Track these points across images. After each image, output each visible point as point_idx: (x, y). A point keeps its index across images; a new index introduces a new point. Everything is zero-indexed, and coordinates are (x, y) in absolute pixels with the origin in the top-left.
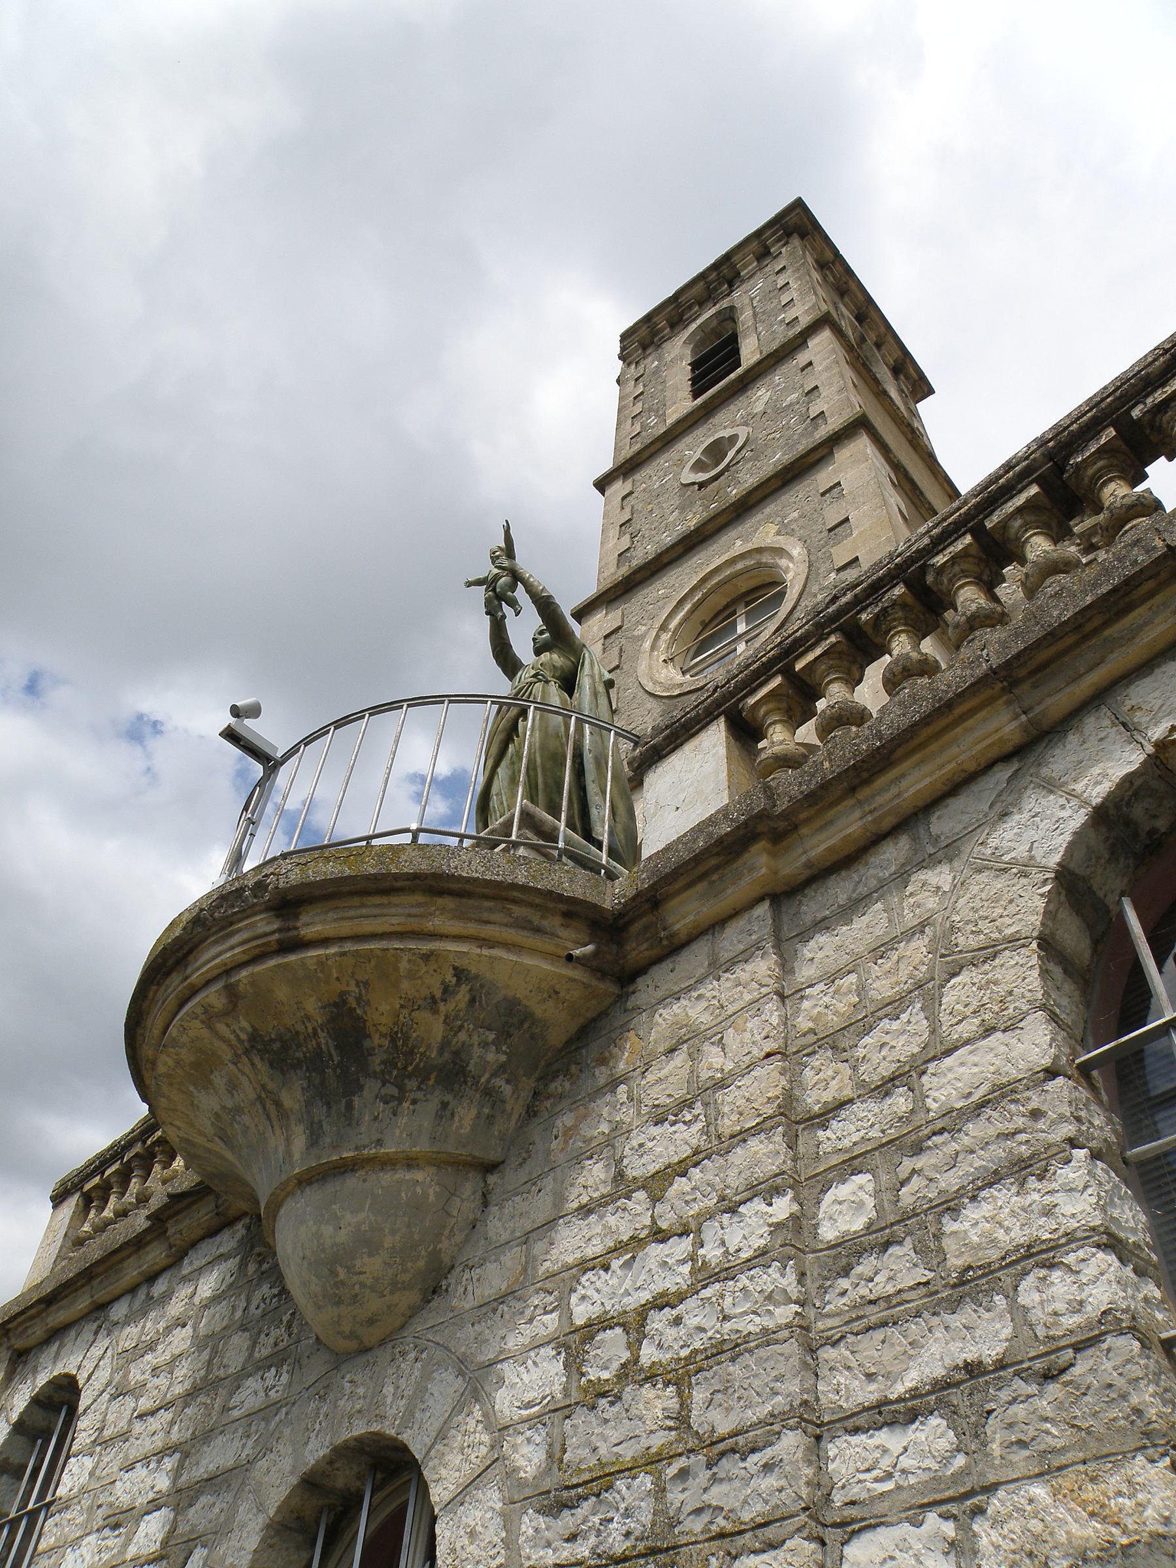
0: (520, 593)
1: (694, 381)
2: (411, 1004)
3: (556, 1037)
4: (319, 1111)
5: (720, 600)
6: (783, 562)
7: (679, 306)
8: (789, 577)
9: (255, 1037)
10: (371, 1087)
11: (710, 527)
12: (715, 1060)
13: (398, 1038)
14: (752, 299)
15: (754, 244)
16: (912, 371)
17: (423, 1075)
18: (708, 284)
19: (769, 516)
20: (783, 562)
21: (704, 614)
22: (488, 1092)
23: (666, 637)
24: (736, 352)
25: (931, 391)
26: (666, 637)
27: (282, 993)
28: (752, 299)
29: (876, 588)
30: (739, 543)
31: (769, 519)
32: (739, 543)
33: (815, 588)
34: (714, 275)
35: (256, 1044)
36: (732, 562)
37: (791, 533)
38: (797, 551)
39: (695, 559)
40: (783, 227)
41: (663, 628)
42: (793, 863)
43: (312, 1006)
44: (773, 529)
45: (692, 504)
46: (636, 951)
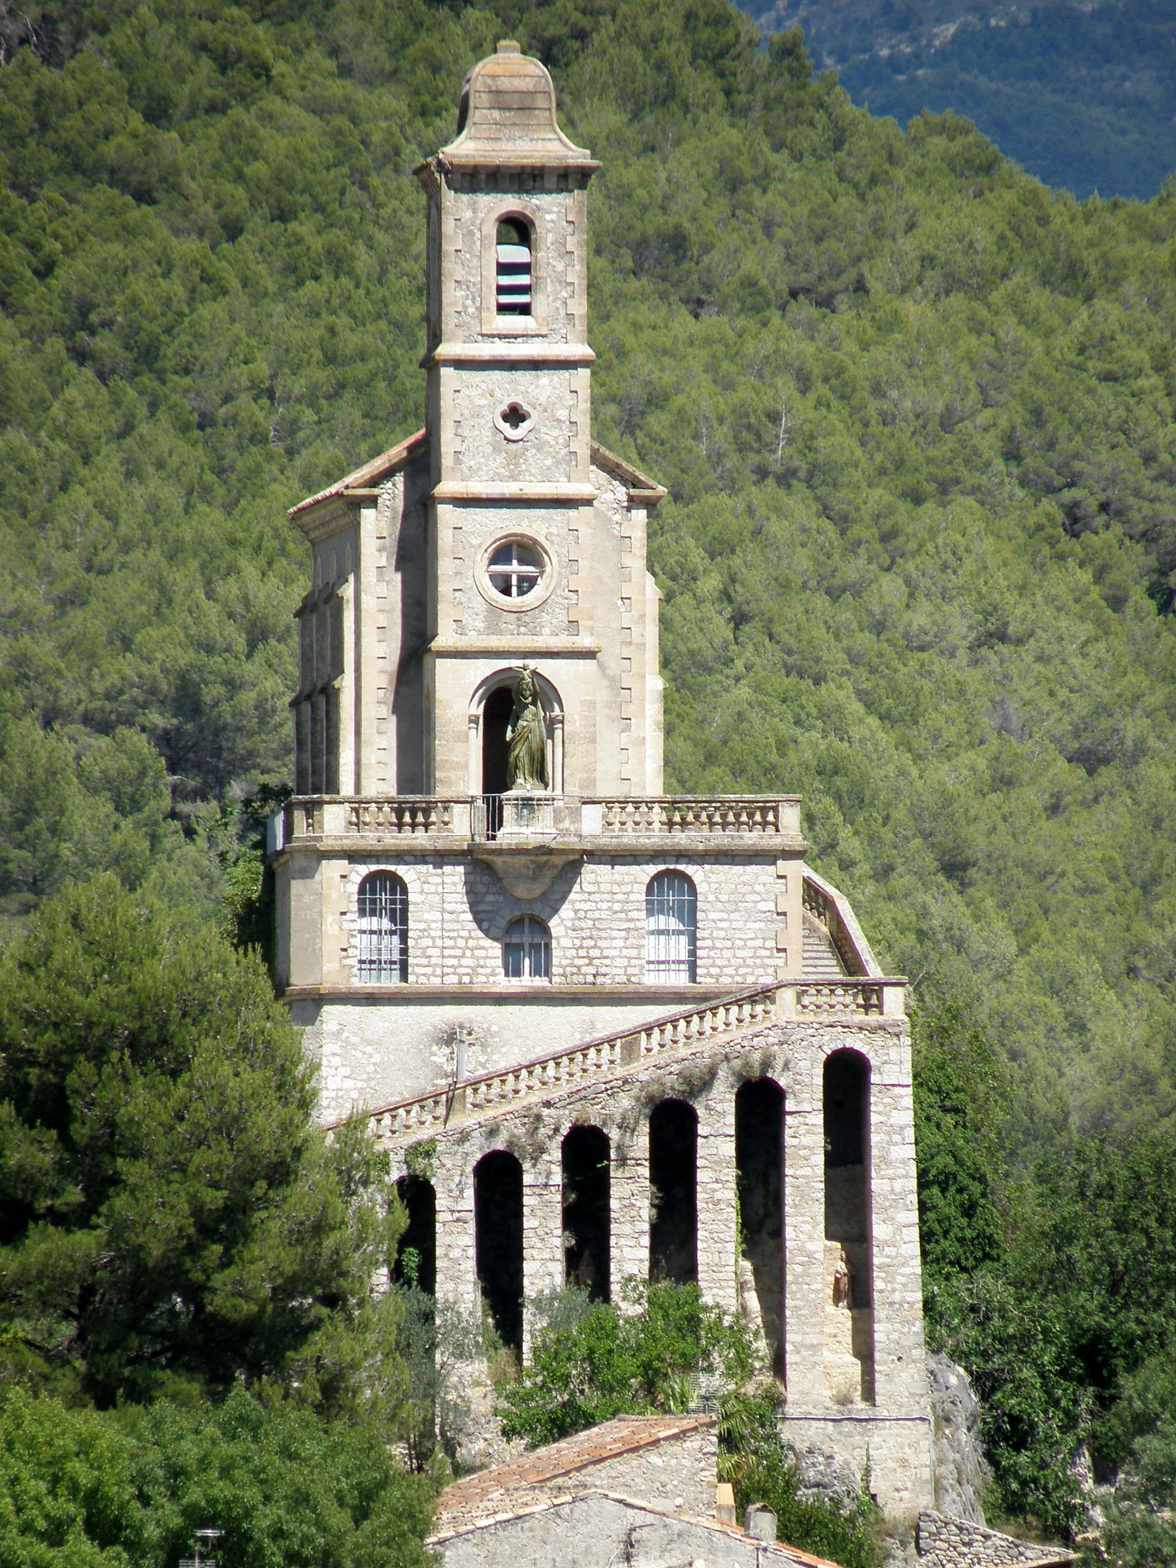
23: (486, 555)
36: (522, 535)
37: (552, 543)
38: (554, 561)
44: (544, 531)
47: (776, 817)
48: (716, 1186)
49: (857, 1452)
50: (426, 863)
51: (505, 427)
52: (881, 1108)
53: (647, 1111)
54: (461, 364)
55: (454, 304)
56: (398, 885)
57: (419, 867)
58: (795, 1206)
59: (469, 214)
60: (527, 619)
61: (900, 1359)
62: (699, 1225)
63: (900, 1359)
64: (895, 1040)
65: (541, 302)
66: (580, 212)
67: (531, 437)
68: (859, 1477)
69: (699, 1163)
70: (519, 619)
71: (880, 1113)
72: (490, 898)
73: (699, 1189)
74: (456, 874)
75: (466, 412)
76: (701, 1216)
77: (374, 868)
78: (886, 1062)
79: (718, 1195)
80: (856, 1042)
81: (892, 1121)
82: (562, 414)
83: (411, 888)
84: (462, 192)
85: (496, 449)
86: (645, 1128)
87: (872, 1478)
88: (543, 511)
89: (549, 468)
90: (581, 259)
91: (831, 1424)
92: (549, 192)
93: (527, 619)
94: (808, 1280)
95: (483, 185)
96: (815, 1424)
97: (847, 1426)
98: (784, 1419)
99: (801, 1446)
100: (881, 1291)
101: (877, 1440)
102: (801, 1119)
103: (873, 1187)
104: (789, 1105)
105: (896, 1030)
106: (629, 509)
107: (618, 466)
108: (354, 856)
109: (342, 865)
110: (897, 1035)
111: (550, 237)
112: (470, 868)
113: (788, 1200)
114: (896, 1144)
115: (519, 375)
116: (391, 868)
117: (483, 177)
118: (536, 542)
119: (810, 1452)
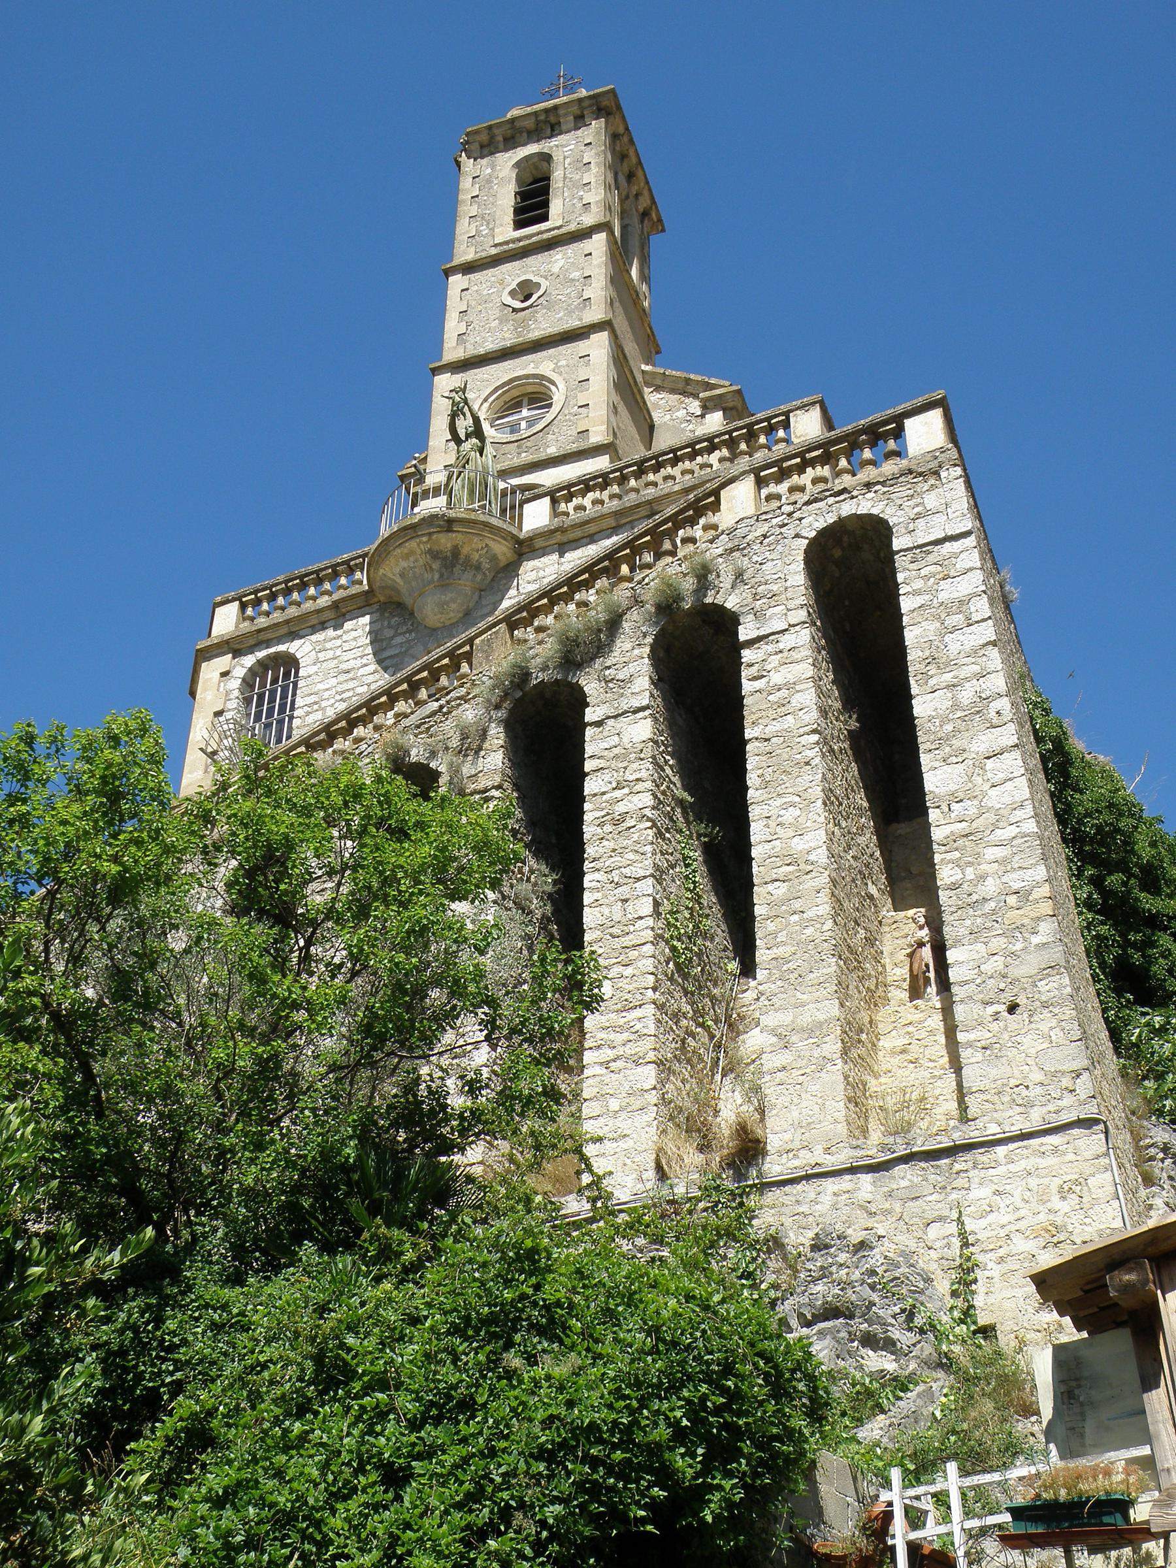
0: (466, 409)
1: (518, 211)
2: (473, 550)
3: (502, 564)
4: (444, 570)
5: (516, 393)
6: (553, 388)
7: (513, 128)
8: (555, 398)
9: (430, 550)
10: (458, 567)
11: (518, 348)
12: (541, 573)
13: (467, 557)
14: (565, 158)
15: (575, 109)
16: (654, 216)
17: (471, 566)
18: (538, 122)
19: (550, 357)
20: (553, 388)
21: (507, 397)
22: (484, 574)
23: (486, 405)
24: (545, 204)
25: (663, 230)
26: (486, 405)
27: (443, 541)
28: (565, 158)
29: (595, 477)
30: (532, 365)
31: (550, 358)
32: (532, 365)
33: (566, 412)
34: (542, 117)
35: (430, 551)
36: (527, 377)
37: (560, 374)
38: (561, 386)
39: (506, 363)
40: (597, 104)
41: (485, 400)
42: (565, 539)
43: (449, 545)
45: (507, 321)
46: (525, 550)
47: (789, 434)
48: (618, 794)
49: (934, 1232)
50: (324, 629)
51: (518, 305)
52: (918, 584)
53: (502, 714)
54: (469, 268)
55: (468, 232)
56: (290, 663)
57: (314, 638)
58: (766, 785)
59: (489, 171)
60: (529, 444)
61: (1012, 1008)
62: (587, 865)
63: (1012, 1008)
64: (932, 481)
65: (556, 207)
66: (598, 133)
67: (539, 302)
68: (943, 1286)
69: (588, 766)
70: (518, 447)
71: (916, 593)
72: (399, 640)
73: (587, 806)
74: (359, 628)
75: (473, 303)
76: (590, 851)
77: (261, 654)
78: (918, 516)
79: (621, 808)
80: (866, 505)
81: (943, 596)
82: (576, 275)
83: (302, 663)
84: (482, 158)
85: (502, 320)
86: (497, 736)
87: (979, 1287)
88: (551, 351)
89: (561, 319)
90: (598, 164)
91: (866, 1179)
92: (569, 131)
93: (529, 444)
94: (797, 905)
95: (501, 146)
96: (831, 1185)
97: (904, 1175)
98: (764, 1187)
99: (798, 1239)
100: (954, 887)
101: (980, 1193)
102: (770, 648)
103: (917, 711)
104: (745, 632)
105: (934, 465)
106: (703, 416)
107: (688, 381)
108: (235, 647)
109: (224, 661)
110: (936, 473)
111: (568, 161)
112: (377, 615)
113: (752, 779)
114: (955, 629)
115: (531, 260)
116: (282, 648)
117: (500, 138)
118: (543, 377)
119: (819, 1246)
